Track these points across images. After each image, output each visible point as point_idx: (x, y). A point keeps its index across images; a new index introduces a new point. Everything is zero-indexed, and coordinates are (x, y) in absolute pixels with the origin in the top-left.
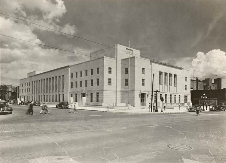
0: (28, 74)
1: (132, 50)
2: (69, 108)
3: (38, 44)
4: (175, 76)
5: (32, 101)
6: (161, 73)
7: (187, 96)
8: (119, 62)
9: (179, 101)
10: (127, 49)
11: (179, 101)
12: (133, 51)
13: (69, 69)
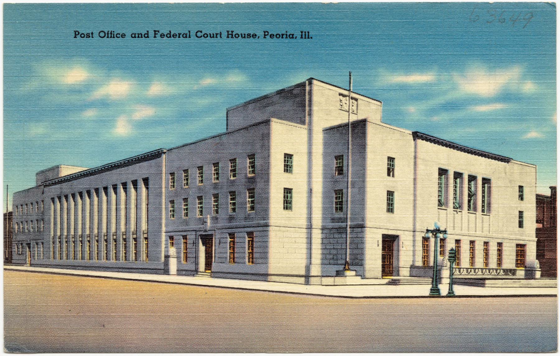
0: (37, 174)
1: (356, 100)
2: (304, 278)
3: (269, 226)
4: (486, 181)
5: (213, 270)
6: (443, 172)
7: (524, 246)
8: (319, 138)
9: (500, 263)
10: (340, 94)
11: (500, 263)
12: (359, 101)
13: (164, 155)
